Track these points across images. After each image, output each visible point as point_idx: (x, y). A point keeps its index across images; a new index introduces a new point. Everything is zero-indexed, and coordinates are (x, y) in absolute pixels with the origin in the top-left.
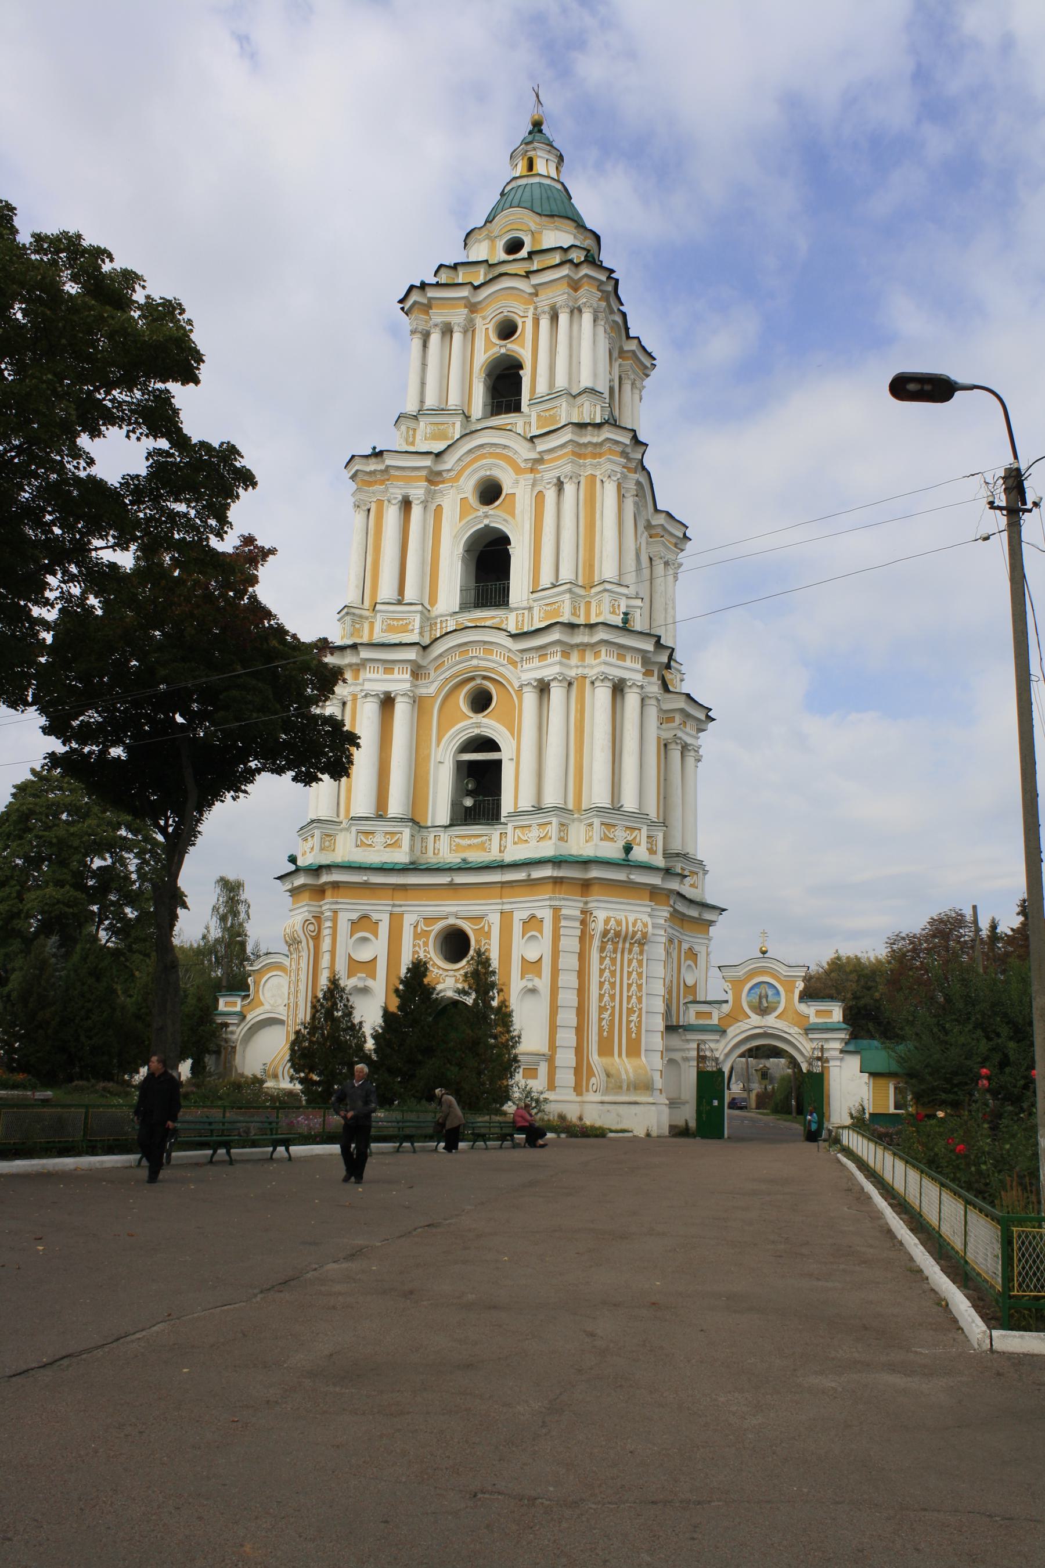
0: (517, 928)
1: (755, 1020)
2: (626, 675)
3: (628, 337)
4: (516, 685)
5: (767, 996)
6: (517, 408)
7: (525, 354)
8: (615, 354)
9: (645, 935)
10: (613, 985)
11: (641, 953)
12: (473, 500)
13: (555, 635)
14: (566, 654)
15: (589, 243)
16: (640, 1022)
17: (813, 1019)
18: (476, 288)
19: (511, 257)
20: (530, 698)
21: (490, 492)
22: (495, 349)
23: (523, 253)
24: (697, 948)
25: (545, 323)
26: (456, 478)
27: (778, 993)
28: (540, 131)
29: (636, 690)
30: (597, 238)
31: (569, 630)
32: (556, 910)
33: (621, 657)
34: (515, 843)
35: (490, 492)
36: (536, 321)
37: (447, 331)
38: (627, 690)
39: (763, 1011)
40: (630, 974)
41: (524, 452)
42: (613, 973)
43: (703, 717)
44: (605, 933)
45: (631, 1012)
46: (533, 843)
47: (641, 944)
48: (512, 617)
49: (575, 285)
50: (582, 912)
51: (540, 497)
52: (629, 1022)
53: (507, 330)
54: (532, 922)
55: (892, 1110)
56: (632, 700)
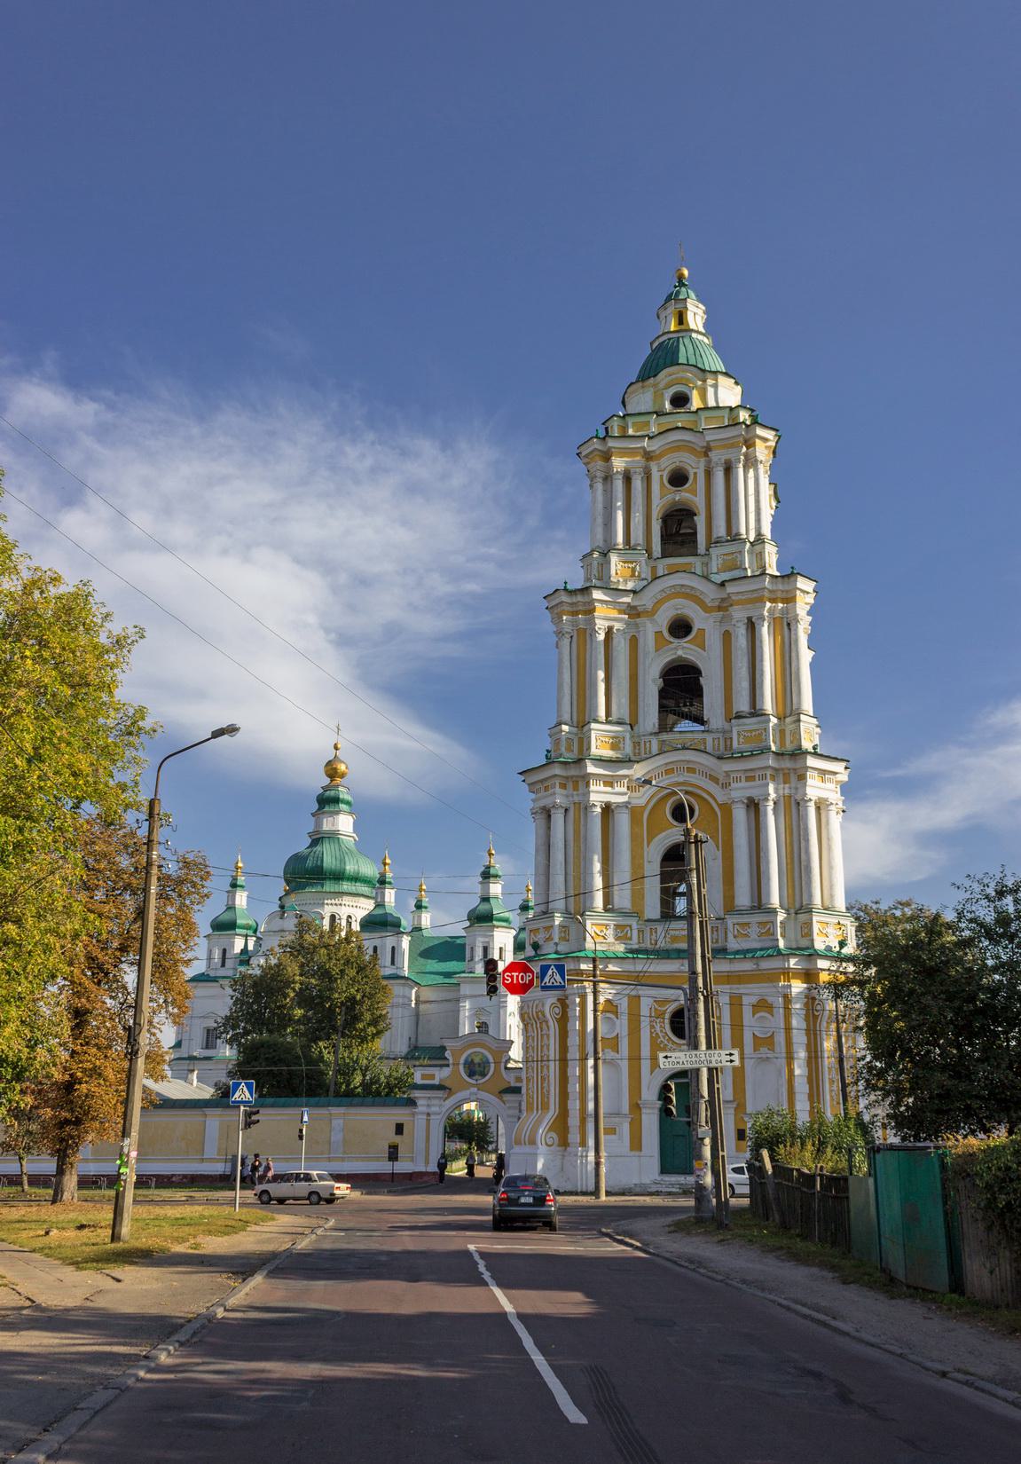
0: (747, 1012)
2: (824, 795)
4: (721, 798)
7: (699, 502)
12: (666, 634)
20: (740, 815)
21: (681, 628)
22: (670, 497)
25: (719, 476)
26: (650, 614)
35: (681, 628)
37: (627, 478)
41: (710, 593)
46: (754, 936)
48: (709, 738)
51: (727, 637)
53: (678, 479)
54: (762, 1006)
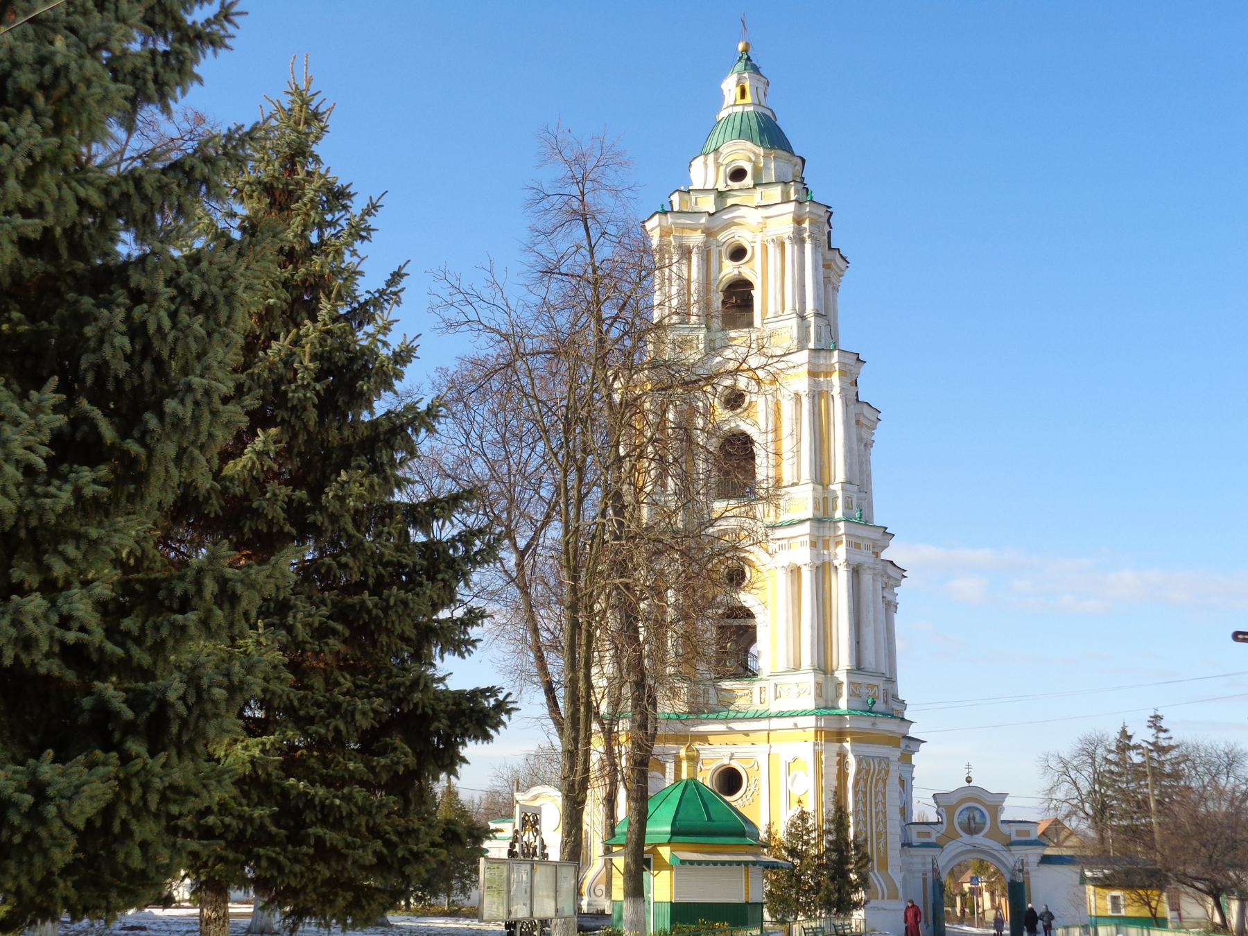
1: (966, 837)
3: (830, 248)
5: (974, 818)
6: (750, 324)
8: (821, 263)
9: (887, 773)
10: (865, 813)
11: (884, 787)
13: (806, 528)
14: (813, 544)
15: (799, 167)
16: (886, 843)
17: (1014, 838)
18: (711, 215)
19: (736, 185)
23: (748, 181)
24: (905, 776)
27: (983, 815)
28: (748, 59)
29: (868, 571)
30: (803, 161)
31: (816, 525)
32: (817, 755)
33: (858, 546)
34: (776, 698)
36: (765, 249)
38: (861, 571)
39: (971, 829)
40: (877, 804)
42: (865, 804)
43: (899, 577)
44: (858, 772)
45: (879, 834)
47: (884, 781)
49: (798, 221)
50: (839, 755)
52: (878, 843)
55: (1110, 913)
56: (867, 578)
